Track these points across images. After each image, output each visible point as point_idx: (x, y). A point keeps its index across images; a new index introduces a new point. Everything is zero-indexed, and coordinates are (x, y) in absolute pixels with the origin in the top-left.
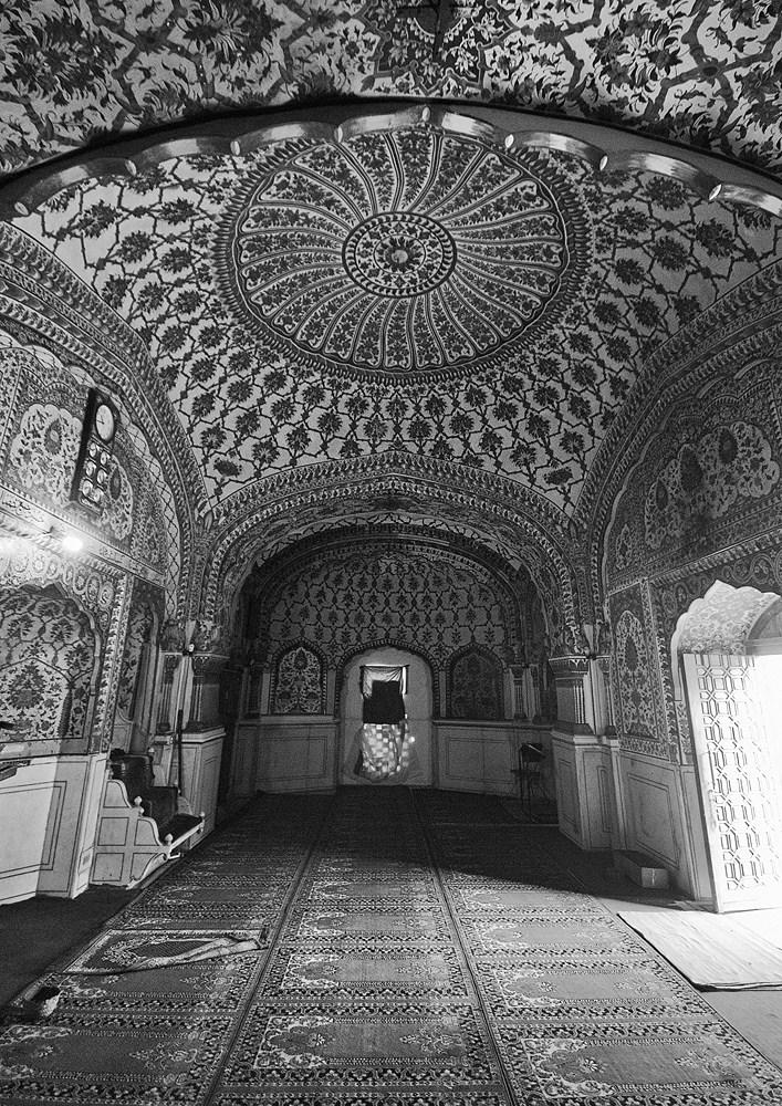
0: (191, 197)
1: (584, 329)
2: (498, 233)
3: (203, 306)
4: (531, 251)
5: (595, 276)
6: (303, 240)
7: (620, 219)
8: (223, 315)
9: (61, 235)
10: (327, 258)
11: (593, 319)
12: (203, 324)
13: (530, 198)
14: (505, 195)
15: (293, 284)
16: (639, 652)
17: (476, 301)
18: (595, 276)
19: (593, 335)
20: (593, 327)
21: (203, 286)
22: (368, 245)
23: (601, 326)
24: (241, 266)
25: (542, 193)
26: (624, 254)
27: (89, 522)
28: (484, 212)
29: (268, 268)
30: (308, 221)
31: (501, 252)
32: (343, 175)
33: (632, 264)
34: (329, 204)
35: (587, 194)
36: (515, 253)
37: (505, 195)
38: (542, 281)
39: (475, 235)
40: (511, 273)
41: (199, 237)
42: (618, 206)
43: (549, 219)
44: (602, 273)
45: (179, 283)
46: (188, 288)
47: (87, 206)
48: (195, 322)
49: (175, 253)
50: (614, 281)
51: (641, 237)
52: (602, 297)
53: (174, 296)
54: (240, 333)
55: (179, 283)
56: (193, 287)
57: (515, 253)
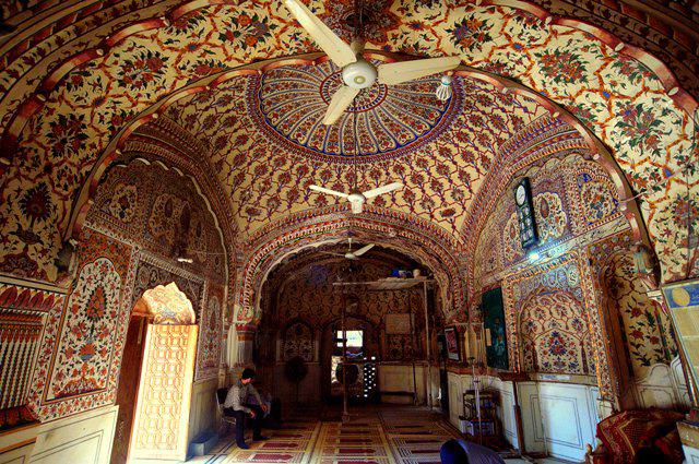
0: (436, 154)
1: (230, 106)
2: (304, 113)
3: (473, 113)
4: (284, 111)
5: (251, 126)
6: (405, 107)
7: (263, 150)
8: (468, 102)
9: (471, 191)
10: (396, 94)
11: (233, 113)
12: (482, 108)
13: (299, 135)
14: (309, 132)
15: (421, 88)
16: (108, 305)
17: (300, 76)
18: (251, 126)
19: (224, 109)
20: (228, 111)
21: (464, 119)
22: (372, 96)
23: (226, 116)
24: (442, 113)
25: (296, 141)
26: (250, 142)
27: (538, 247)
28: (314, 120)
29: (430, 101)
30: (400, 115)
31: (298, 105)
32: (378, 133)
33: (244, 143)
34: (387, 120)
35: (281, 151)
36: (291, 107)
37: (309, 132)
38: (269, 103)
39: (315, 107)
40: (287, 98)
41: (447, 138)
42: (268, 154)
43: (287, 132)
44: (249, 129)
45: (471, 130)
46: (471, 125)
47: (461, 183)
48: (483, 113)
49: (461, 140)
50: (242, 132)
51: (252, 152)
52: (239, 123)
53: (479, 129)
54: (467, 89)
55: (471, 130)
56: (468, 123)
57: (291, 107)
